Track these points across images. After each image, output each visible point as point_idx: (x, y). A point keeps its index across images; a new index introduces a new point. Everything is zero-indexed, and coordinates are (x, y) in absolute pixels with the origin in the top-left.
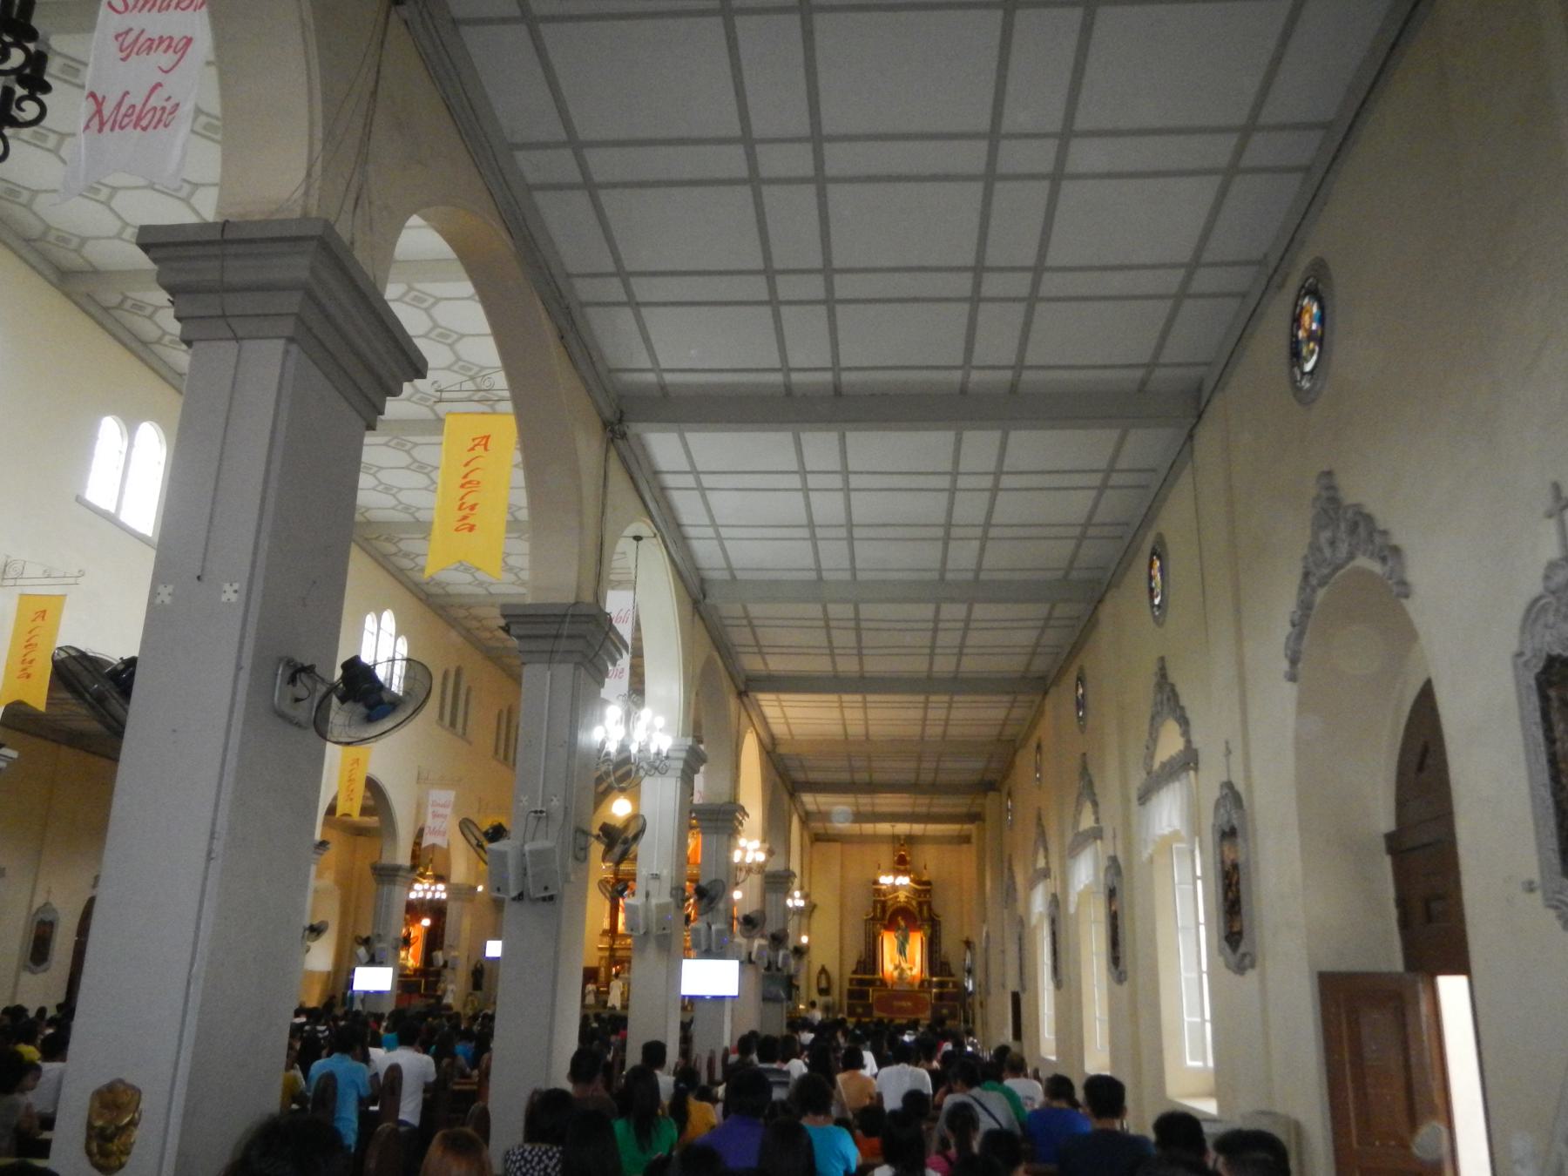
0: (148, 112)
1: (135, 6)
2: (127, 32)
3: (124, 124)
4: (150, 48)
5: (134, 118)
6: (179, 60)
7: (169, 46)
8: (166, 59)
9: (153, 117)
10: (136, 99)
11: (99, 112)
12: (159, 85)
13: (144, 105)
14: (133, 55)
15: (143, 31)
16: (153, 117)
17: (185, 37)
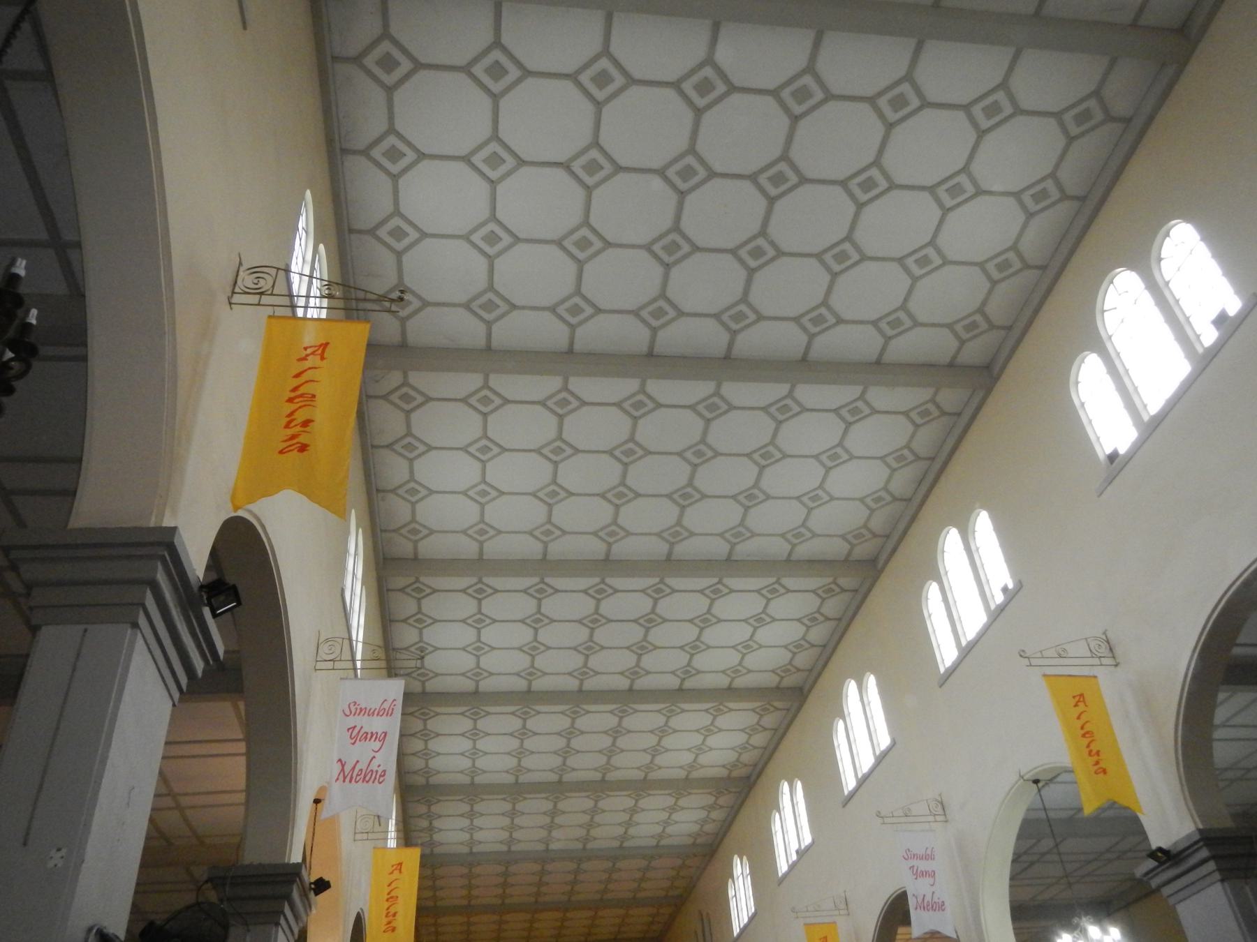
1: (354, 715)
2: (355, 727)
3: (357, 780)
4: (366, 738)
5: (362, 776)
6: (382, 745)
7: (376, 738)
8: (377, 745)
9: (372, 775)
11: (343, 770)
12: (374, 757)
13: (367, 768)
14: (358, 741)
15: (362, 727)
16: (372, 775)
17: (383, 732)
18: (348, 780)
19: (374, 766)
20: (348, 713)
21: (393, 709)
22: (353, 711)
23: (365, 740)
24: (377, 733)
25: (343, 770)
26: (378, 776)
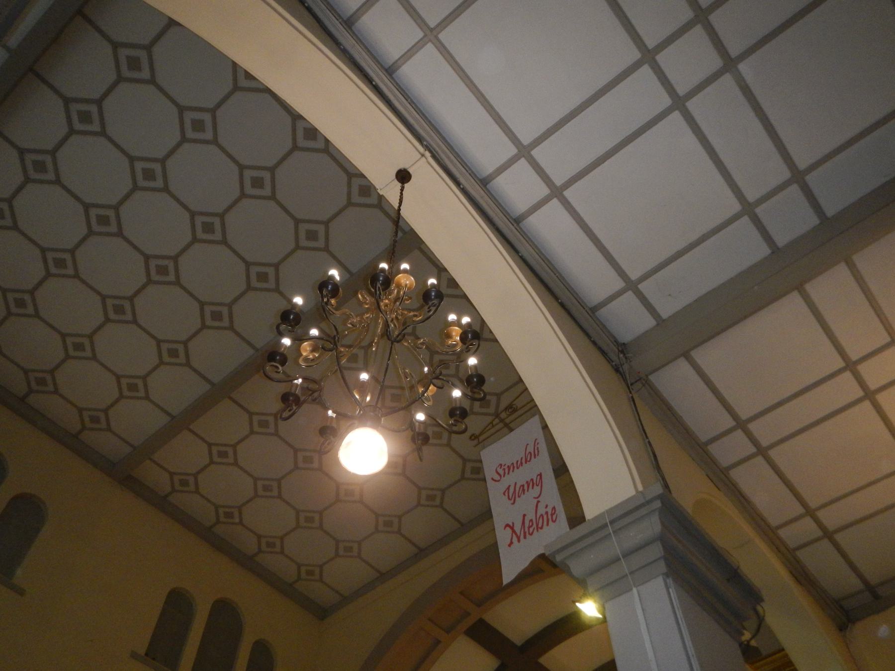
0: (539, 518)
1: (505, 473)
2: (508, 488)
4: (524, 490)
5: (535, 525)
8: (537, 489)
10: (531, 516)
11: (514, 531)
12: (538, 502)
13: (536, 516)
14: (517, 499)
15: (516, 484)
18: (522, 537)
19: (542, 510)
20: (497, 477)
21: (538, 448)
22: (502, 476)
23: (524, 494)
24: (532, 480)
25: (514, 531)
26: (550, 517)
